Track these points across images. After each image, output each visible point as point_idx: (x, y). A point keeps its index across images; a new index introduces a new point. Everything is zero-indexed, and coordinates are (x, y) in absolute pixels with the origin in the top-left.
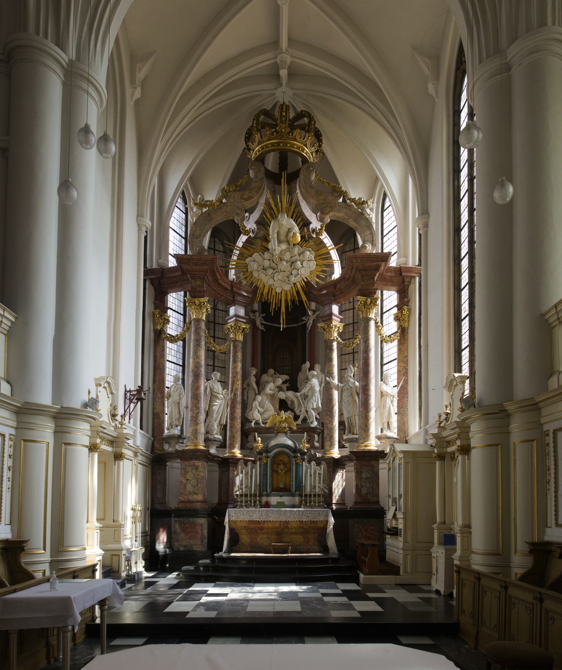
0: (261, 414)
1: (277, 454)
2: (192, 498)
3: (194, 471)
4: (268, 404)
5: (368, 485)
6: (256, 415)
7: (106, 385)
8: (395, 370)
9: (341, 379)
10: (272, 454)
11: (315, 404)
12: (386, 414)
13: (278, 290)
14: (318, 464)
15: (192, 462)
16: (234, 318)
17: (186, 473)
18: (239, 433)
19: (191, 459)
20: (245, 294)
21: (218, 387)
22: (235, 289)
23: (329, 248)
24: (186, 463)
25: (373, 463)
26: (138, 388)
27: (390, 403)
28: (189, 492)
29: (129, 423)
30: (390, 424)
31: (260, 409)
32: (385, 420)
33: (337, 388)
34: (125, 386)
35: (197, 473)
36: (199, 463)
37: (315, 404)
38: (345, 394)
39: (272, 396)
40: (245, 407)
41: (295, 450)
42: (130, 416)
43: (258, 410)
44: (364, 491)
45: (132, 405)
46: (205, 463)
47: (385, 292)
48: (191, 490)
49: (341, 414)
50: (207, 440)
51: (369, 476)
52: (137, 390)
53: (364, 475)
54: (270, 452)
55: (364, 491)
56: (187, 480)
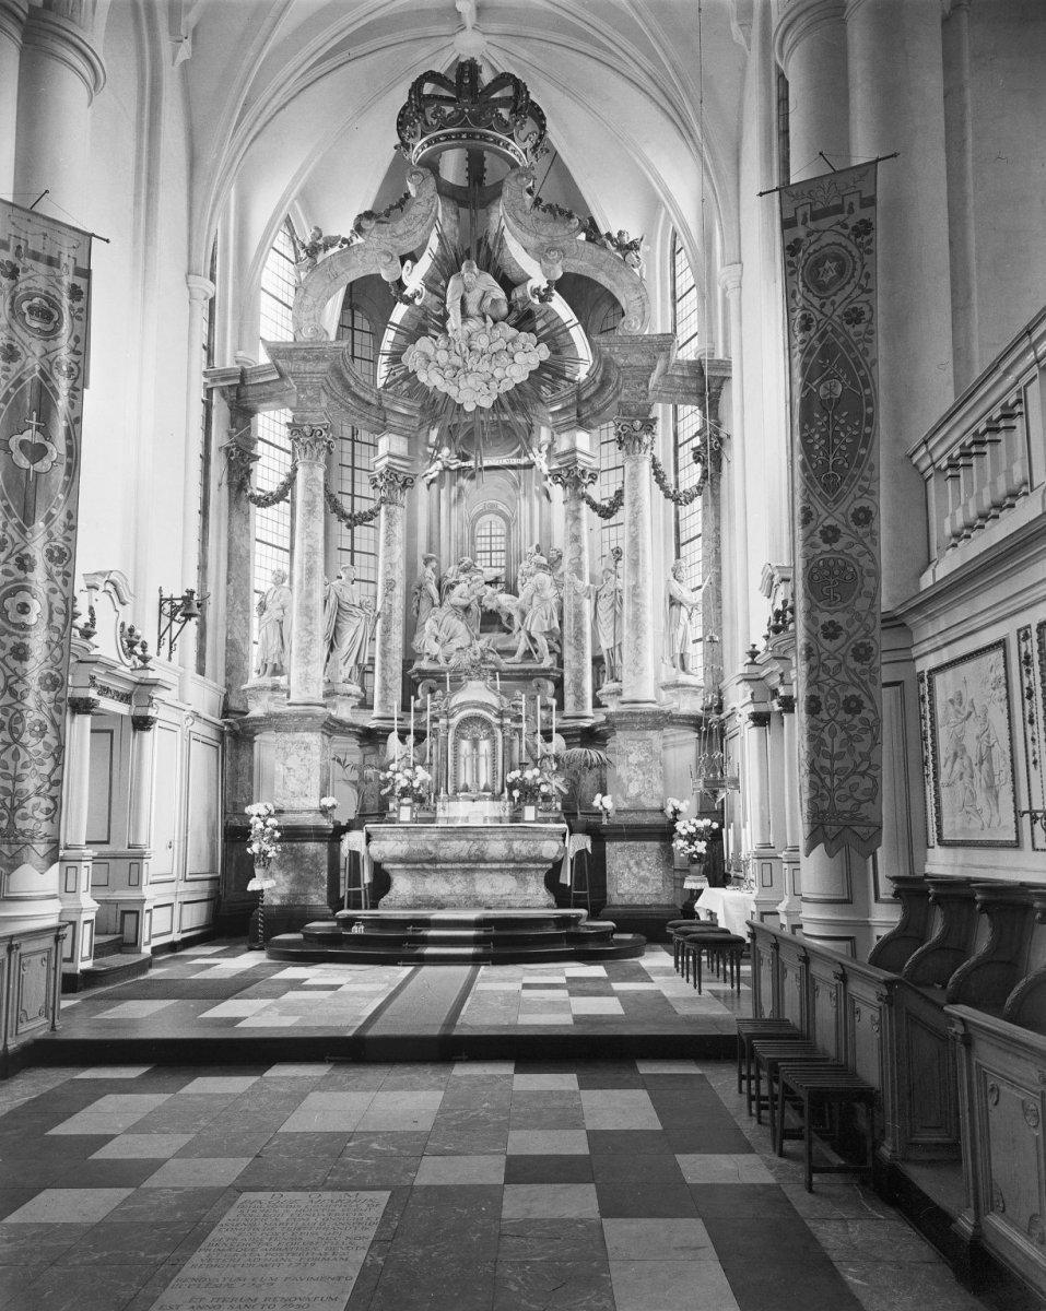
0: (443, 645)
2: (297, 804)
3: (302, 752)
4: (459, 626)
5: (641, 777)
7: (110, 587)
8: (699, 556)
15: (298, 736)
16: (387, 460)
17: (287, 756)
20: (404, 411)
22: (386, 404)
23: (568, 325)
24: (287, 737)
26: (186, 594)
27: (686, 618)
28: (293, 793)
29: (170, 659)
30: (685, 657)
34: (160, 590)
35: (309, 756)
40: (411, 628)
42: (171, 647)
45: (176, 627)
46: (326, 737)
47: (680, 407)
51: (642, 759)
52: (183, 598)
54: (452, 716)
56: (289, 769)
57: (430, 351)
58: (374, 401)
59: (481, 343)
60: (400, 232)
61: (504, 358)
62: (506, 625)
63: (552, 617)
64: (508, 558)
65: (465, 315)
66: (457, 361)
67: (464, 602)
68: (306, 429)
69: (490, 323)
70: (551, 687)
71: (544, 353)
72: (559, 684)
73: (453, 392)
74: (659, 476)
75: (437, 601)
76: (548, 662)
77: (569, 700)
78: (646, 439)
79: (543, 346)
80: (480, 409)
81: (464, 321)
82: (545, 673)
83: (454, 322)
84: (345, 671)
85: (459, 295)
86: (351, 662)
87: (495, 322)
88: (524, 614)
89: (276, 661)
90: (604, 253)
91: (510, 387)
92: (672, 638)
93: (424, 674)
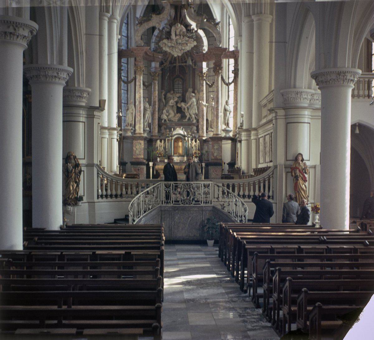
3: (139, 145)
4: (171, 112)
10: (174, 138)
13: (176, 56)
15: (138, 141)
19: (138, 140)
21: (147, 105)
25: (220, 142)
31: (167, 114)
32: (226, 122)
38: (208, 109)
39: (173, 106)
44: (215, 155)
48: (138, 153)
50: (144, 130)
54: (173, 137)
55: (215, 155)
59: (180, 41)
60: (161, 18)
63: (196, 109)
64: (183, 90)
65: (176, 35)
66: (173, 45)
67: (172, 105)
68: (139, 67)
69: (182, 37)
70: (195, 128)
71: (195, 43)
72: (198, 127)
73: (172, 52)
74: (223, 79)
75: (165, 104)
76: (195, 121)
77: (200, 132)
78: (220, 71)
80: (178, 56)
81: (175, 37)
82: (194, 124)
83: (173, 36)
84: (146, 124)
85: (175, 31)
86: (147, 123)
87: (183, 36)
88: (188, 109)
89: (131, 123)
90: (211, 25)
91: (186, 51)
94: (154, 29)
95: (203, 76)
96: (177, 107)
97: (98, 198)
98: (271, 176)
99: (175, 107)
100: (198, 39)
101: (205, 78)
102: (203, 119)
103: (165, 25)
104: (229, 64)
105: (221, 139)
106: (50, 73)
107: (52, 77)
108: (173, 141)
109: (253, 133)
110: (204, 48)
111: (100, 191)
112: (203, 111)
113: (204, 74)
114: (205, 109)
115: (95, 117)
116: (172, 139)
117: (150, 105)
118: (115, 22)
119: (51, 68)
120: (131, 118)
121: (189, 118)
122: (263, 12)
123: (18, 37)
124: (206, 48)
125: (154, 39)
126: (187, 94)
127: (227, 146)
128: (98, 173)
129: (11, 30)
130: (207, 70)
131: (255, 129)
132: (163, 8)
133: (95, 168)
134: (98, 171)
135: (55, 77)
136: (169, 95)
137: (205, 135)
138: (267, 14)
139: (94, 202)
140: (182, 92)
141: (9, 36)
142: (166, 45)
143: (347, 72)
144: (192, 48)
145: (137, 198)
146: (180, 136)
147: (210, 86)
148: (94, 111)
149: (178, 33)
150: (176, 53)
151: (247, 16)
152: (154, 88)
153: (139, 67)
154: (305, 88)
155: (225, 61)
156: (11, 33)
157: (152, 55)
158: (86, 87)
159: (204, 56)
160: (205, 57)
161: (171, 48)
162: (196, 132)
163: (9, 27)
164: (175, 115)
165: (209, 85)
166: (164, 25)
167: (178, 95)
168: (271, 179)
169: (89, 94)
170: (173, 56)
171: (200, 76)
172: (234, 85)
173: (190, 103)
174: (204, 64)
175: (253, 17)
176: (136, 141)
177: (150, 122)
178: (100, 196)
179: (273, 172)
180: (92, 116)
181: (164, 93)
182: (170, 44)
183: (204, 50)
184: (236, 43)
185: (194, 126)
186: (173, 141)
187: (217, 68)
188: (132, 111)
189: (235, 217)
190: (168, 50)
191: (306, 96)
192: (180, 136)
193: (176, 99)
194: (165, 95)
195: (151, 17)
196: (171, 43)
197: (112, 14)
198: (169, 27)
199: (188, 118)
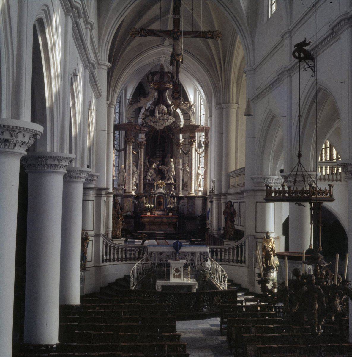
1: (158, 196)
6: (149, 177)
9: (183, 166)
10: (156, 196)
11: (172, 173)
12: (199, 181)
14: (174, 199)
15: (128, 199)
18: (143, 185)
19: (128, 198)
21: (135, 169)
25: (193, 200)
33: (182, 169)
36: (130, 199)
37: (172, 173)
41: (165, 194)
43: (150, 176)
44: (190, 210)
49: (183, 180)
53: (190, 204)
55: (190, 210)
57: (151, 119)
58: (140, 129)
60: (147, 100)
61: (166, 121)
62: (163, 172)
65: (159, 113)
68: (129, 139)
70: (173, 186)
71: (174, 120)
76: (173, 181)
77: (177, 190)
78: (194, 143)
79: (174, 118)
80: (160, 129)
81: (159, 114)
82: (172, 184)
92: (198, 181)
93: (147, 184)
94: (140, 108)
95: (180, 146)
96: (159, 169)
97: (103, 262)
98: (243, 244)
99: (157, 168)
100: (176, 116)
101: (181, 147)
102: (179, 180)
103: (150, 105)
104: (200, 137)
105: (194, 198)
106: (74, 174)
107: (75, 177)
108: (155, 198)
109: (222, 197)
110: (181, 123)
111: (105, 256)
112: (179, 173)
113: (181, 144)
114: (181, 172)
115: (103, 195)
116: (155, 197)
117: (137, 168)
118: (112, 107)
119: (75, 171)
120: (122, 179)
121: (168, 178)
122: (231, 102)
123: (60, 167)
124: (182, 124)
125: (141, 116)
126: (167, 159)
127: (199, 203)
128: (103, 242)
129: (56, 162)
130: (183, 141)
131: (224, 195)
132: (149, 92)
133: (101, 237)
134: (104, 240)
135: (78, 177)
136: (152, 159)
137: (181, 193)
138: (234, 103)
139: (100, 266)
140: (162, 157)
141: (54, 167)
142: (151, 121)
143: (312, 175)
144: (171, 124)
145: (136, 265)
146: (161, 194)
147: (186, 154)
148: (102, 191)
149: (160, 112)
150: (158, 127)
151: (218, 104)
152: (140, 155)
153: (129, 139)
154: (270, 175)
155: (197, 134)
156: (55, 165)
157: (140, 129)
158: (96, 172)
159: (181, 130)
160: (182, 131)
161: (155, 123)
162: (174, 190)
163: (54, 161)
164: (157, 176)
165: (185, 153)
166: (150, 106)
167: (159, 159)
168: (243, 247)
169: (97, 177)
170: (156, 129)
171: (177, 146)
172: (205, 153)
173: (169, 166)
174: (181, 136)
175: (223, 105)
176: (126, 199)
177: (137, 182)
178: (104, 261)
179: (245, 241)
180: (100, 195)
181: (148, 158)
182: (154, 120)
183: (181, 125)
184: (206, 121)
185: (173, 185)
186: (155, 198)
187: (191, 140)
188: (123, 174)
189: (216, 281)
190: (152, 124)
191: (271, 181)
192: (161, 194)
193: (158, 163)
194: (148, 159)
195: (140, 99)
196: (155, 119)
197: (111, 101)
198: (153, 107)
199: (167, 178)
